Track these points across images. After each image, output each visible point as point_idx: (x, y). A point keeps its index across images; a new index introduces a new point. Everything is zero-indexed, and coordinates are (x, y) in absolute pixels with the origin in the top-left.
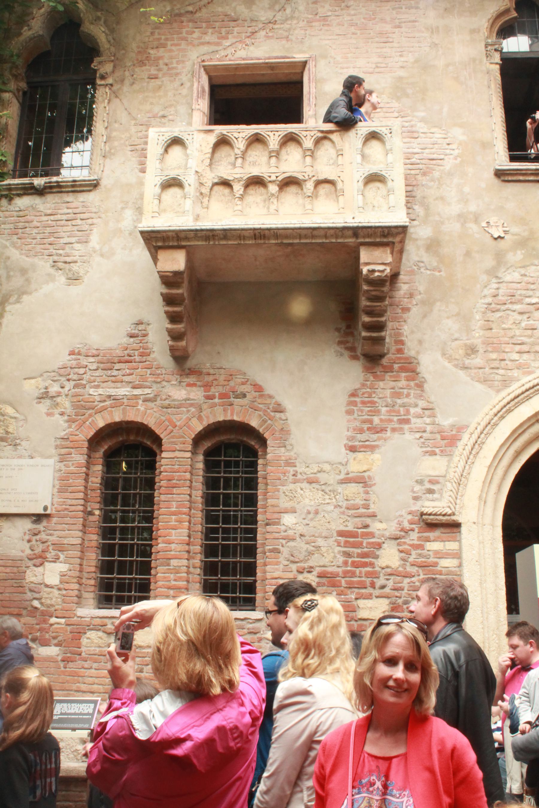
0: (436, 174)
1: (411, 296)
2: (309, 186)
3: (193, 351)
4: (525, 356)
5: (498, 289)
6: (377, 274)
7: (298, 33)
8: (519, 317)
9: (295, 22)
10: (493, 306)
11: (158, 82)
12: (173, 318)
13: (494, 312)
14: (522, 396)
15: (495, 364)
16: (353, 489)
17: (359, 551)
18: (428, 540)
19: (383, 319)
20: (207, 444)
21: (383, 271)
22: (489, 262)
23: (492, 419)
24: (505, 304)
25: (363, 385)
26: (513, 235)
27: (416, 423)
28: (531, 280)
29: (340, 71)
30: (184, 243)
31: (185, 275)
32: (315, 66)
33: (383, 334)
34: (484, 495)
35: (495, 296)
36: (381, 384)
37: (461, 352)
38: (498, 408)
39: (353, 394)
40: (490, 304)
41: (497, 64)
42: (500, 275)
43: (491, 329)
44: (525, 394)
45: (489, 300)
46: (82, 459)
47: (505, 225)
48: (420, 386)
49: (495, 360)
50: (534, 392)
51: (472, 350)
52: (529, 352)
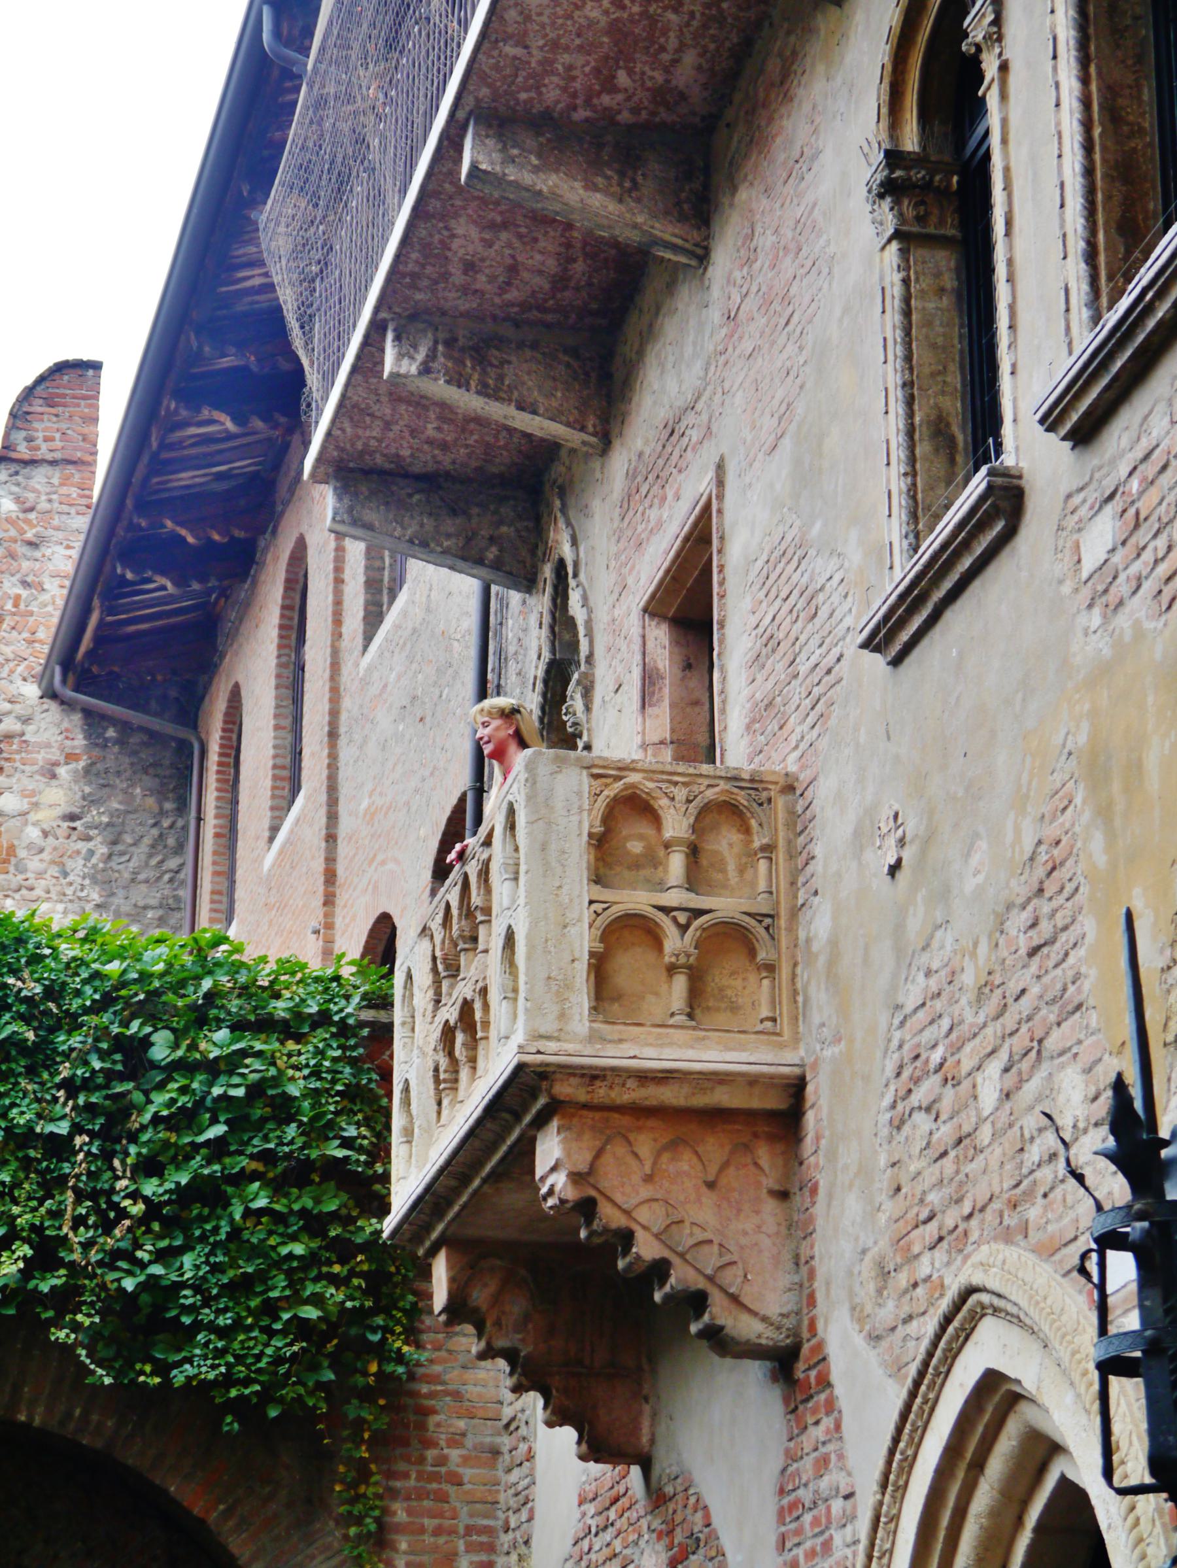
1: (818, 1138)
3: (652, 1441)
4: (940, 1255)
5: (900, 1047)
6: (551, 1202)
7: (718, 398)
9: (713, 368)
10: (900, 1106)
13: (899, 1128)
14: (915, 1408)
15: (906, 1310)
19: (667, 1288)
21: (551, 1192)
23: (881, 1503)
24: (910, 1091)
26: (912, 841)
28: (933, 984)
29: (747, 480)
30: (435, 1235)
31: (480, 1296)
32: (721, 497)
33: (706, 1318)
35: (898, 1074)
36: (804, 1438)
37: (871, 1287)
39: (782, 1492)
40: (893, 1106)
41: (889, 241)
42: (900, 1000)
43: (898, 1189)
44: (919, 1400)
45: (892, 1088)
47: (900, 821)
48: (838, 1427)
49: (906, 1291)
50: (933, 1383)
51: (884, 1274)
52: (941, 1239)
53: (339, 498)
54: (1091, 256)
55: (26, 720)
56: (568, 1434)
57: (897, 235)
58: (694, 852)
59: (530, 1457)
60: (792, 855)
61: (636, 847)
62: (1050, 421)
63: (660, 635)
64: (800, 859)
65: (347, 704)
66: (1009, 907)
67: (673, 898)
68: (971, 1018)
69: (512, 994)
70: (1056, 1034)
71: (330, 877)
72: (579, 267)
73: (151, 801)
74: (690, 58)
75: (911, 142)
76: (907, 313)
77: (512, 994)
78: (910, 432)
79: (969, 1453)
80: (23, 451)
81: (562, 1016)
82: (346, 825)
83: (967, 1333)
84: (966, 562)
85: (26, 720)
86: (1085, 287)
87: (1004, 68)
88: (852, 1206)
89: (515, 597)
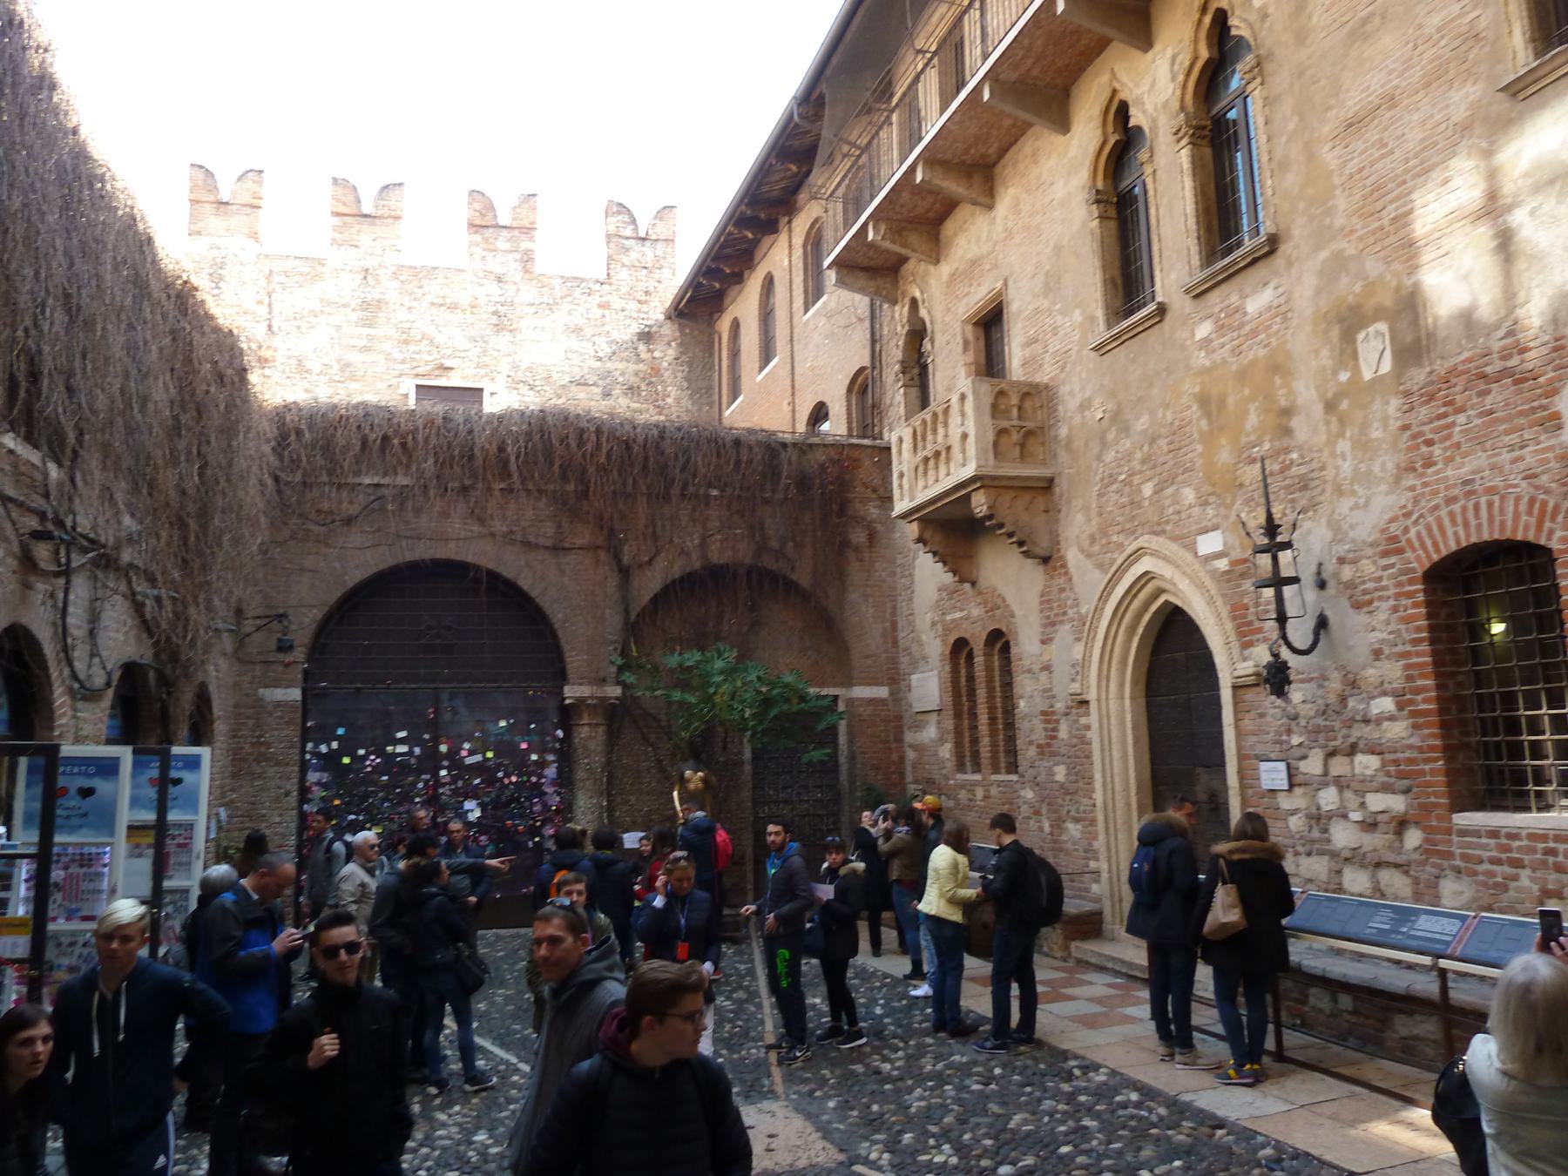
0: (1069, 367)
1: (1061, 496)
2: (943, 454)
7: (1001, 256)
8: (1114, 497)
11: (949, 347)
12: (945, 563)
16: (1044, 676)
17: (1051, 726)
18: (1078, 715)
20: (998, 646)
22: (1095, 447)
25: (1046, 586)
27: (1070, 612)
31: (927, 535)
34: (1105, 672)
38: (1099, 593)
39: (1042, 596)
46: (948, 668)
48: (1070, 580)
51: (1093, 539)
53: (837, 273)
54: (1199, 238)
55: (660, 327)
56: (951, 574)
57: (1099, 217)
58: (1020, 408)
59: (911, 575)
60: (1049, 408)
61: (1003, 407)
62: (1187, 292)
63: (969, 328)
64: (1052, 410)
65: (796, 331)
66: (1159, 436)
67: (1015, 423)
68: (1138, 468)
69: (964, 451)
70: (1180, 478)
71: (793, 387)
72: (938, 205)
73: (701, 354)
74: (996, 145)
75: (1100, 185)
76: (1102, 242)
77: (964, 451)
78: (1105, 281)
79: (1134, 592)
80: (654, 237)
81: (987, 460)
82: (798, 370)
83: (1137, 560)
84: (1141, 329)
85: (660, 327)
86: (1197, 248)
87: (1155, 171)
88: (1080, 518)
89: (886, 306)
